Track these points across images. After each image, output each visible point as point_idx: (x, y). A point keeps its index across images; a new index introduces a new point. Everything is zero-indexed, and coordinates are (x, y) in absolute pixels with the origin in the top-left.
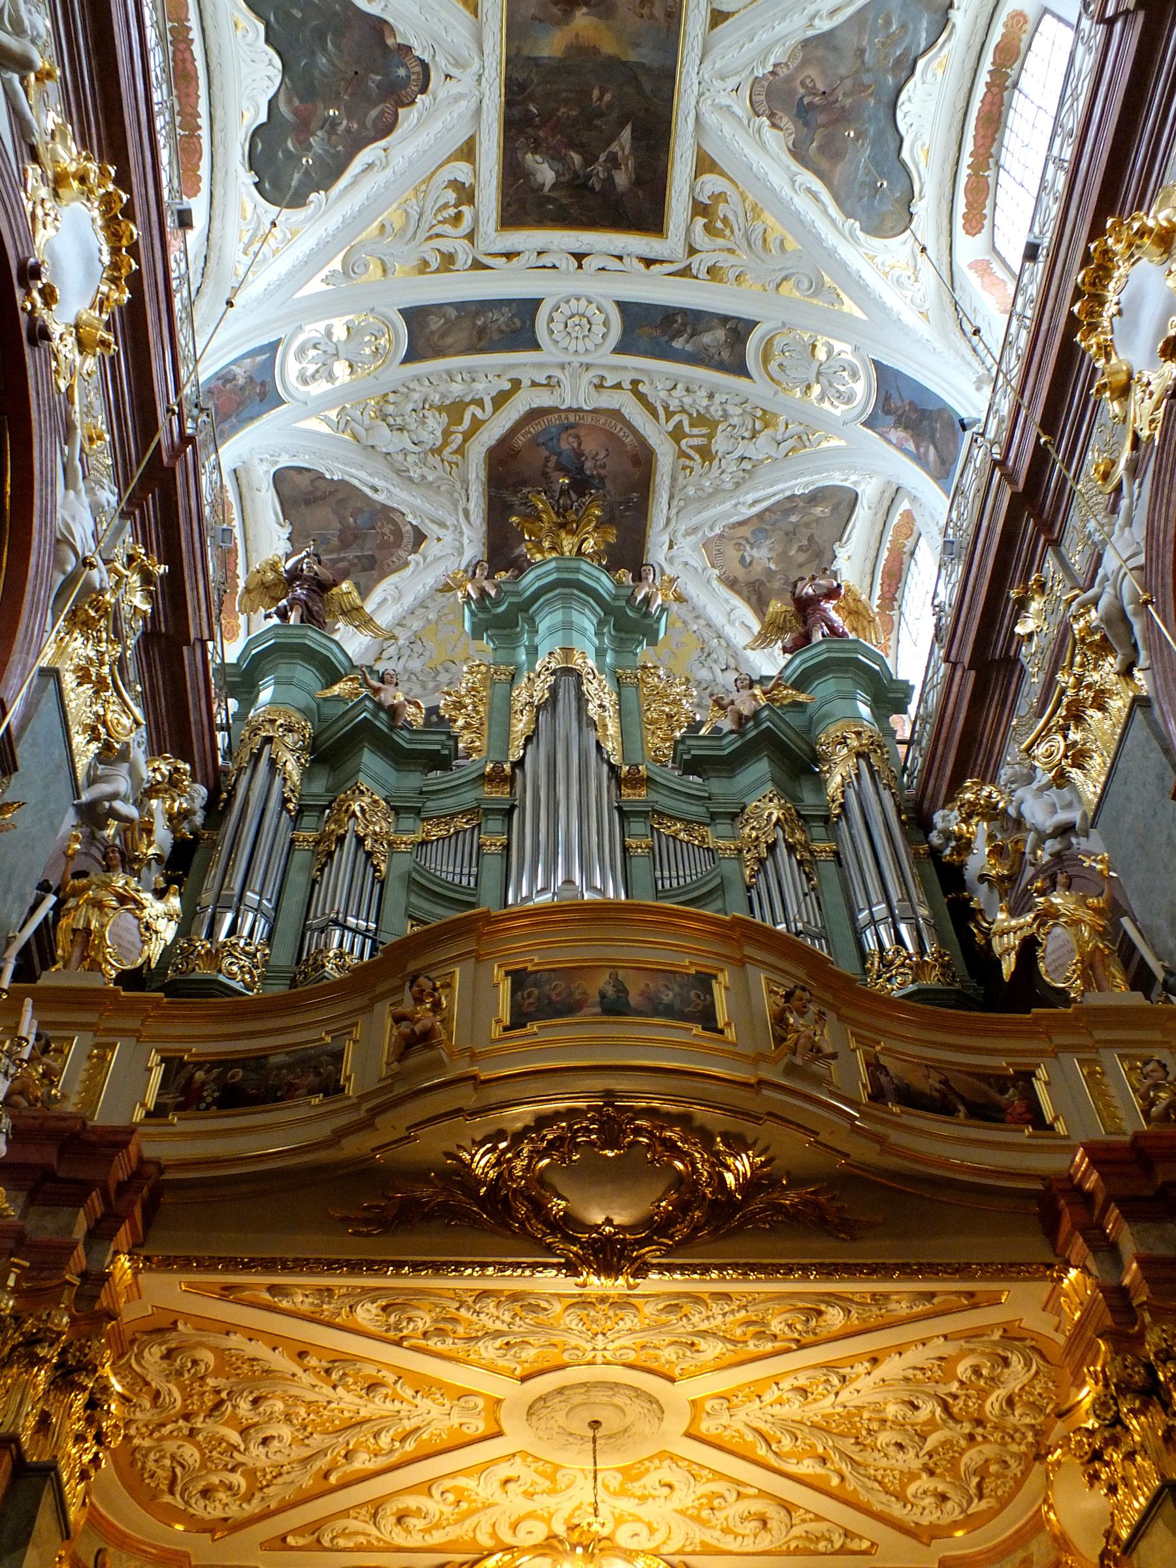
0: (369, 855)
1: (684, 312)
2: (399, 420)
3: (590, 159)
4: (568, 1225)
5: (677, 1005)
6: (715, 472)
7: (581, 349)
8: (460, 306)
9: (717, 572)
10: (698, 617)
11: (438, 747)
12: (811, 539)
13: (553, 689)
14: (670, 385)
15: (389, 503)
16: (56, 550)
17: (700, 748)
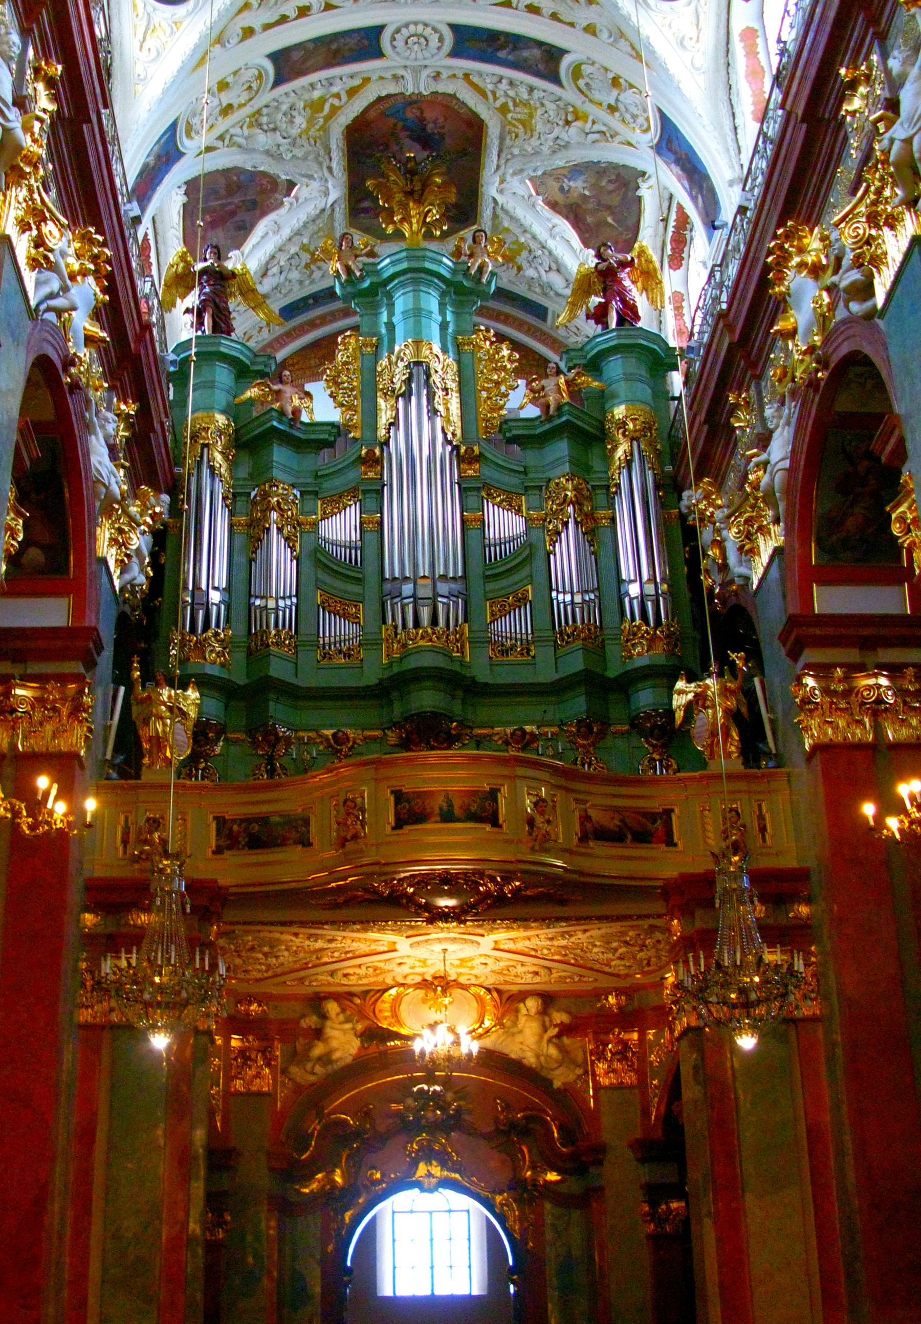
1: (507, 35)
2: (271, 126)
4: (428, 907)
6: (534, 142)
7: (420, 55)
9: (540, 198)
10: (525, 231)
11: (326, 436)
12: (618, 176)
13: (408, 381)
14: (495, 79)
16: (94, 487)
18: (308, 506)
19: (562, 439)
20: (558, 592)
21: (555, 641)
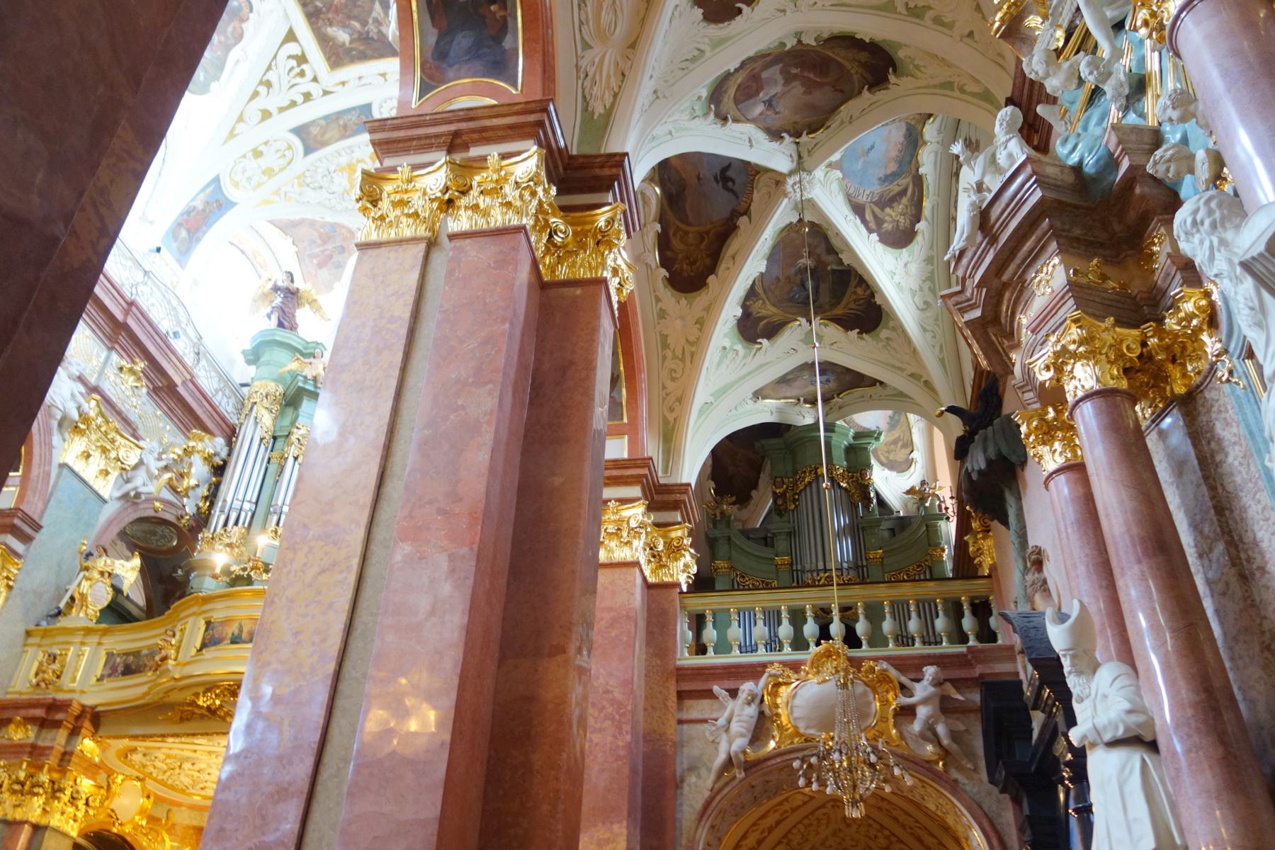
3: (364, 23)
8: (326, 118)
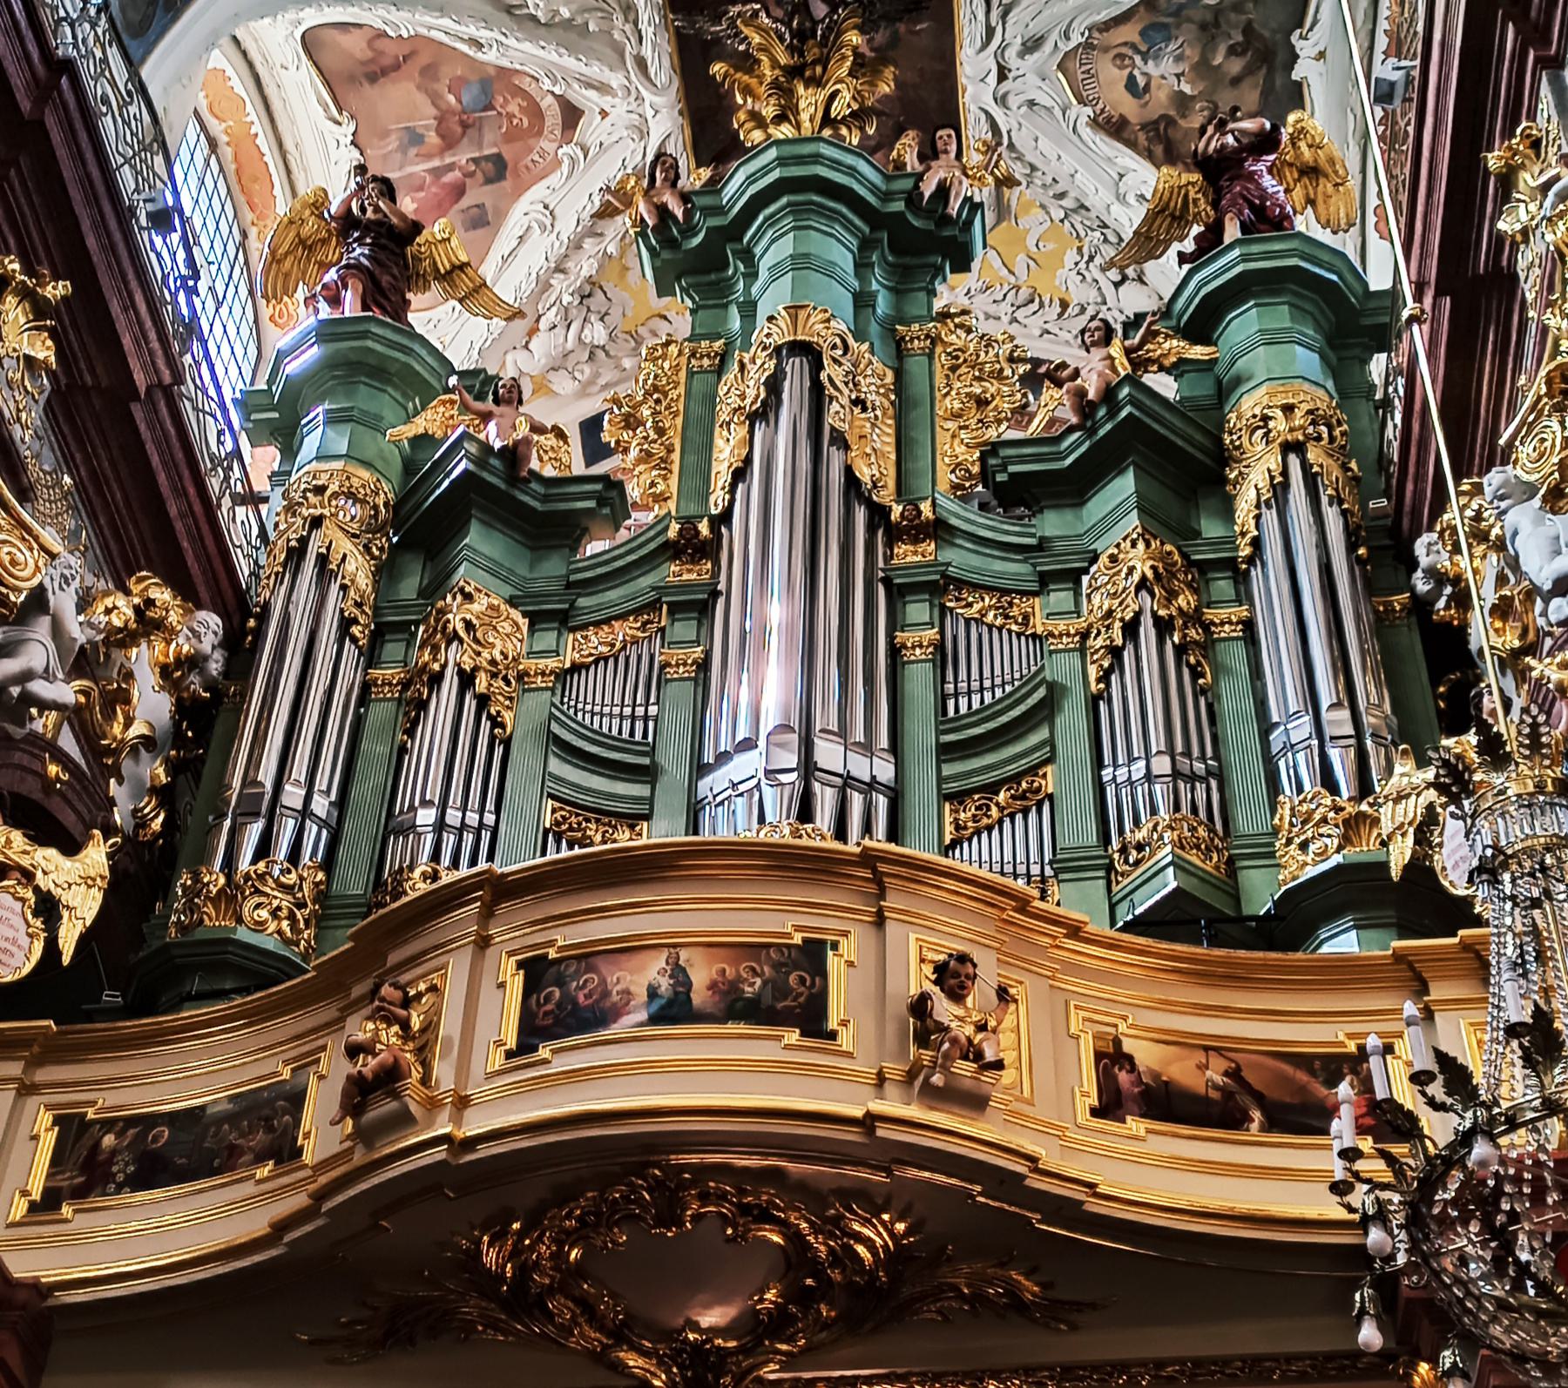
0: (483, 701)
5: (767, 1000)
9: (1089, 111)
15: (505, 63)
17: (1022, 459)
18: (547, 639)
19: (1121, 472)
20: (1116, 766)
21: (1110, 868)
